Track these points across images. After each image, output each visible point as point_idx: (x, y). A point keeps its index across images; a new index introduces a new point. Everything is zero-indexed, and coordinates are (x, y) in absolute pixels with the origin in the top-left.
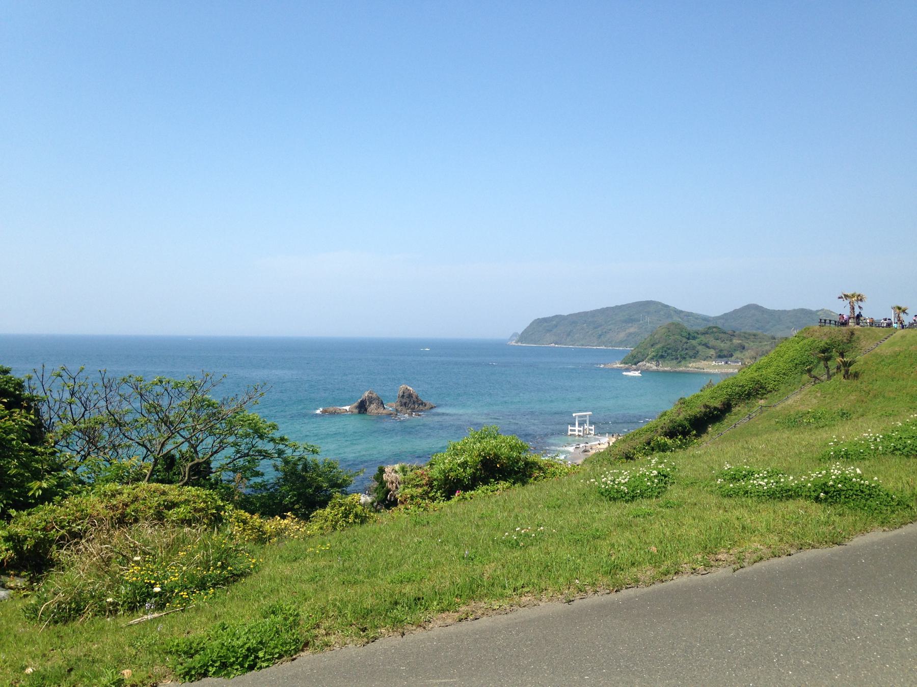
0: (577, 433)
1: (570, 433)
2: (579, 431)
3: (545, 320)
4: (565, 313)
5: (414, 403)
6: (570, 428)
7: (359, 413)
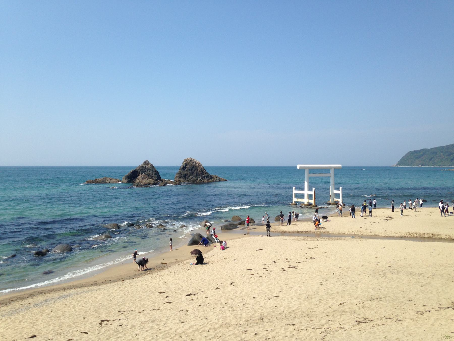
0: (306, 201)
1: (295, 200)
2: (310, 196)
3: (415, 152)
4: (429, 147)
5: (197, 175)
6: (295, 192)
7: (129, 182)
